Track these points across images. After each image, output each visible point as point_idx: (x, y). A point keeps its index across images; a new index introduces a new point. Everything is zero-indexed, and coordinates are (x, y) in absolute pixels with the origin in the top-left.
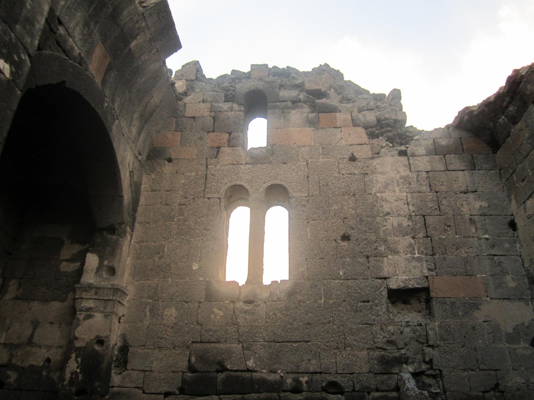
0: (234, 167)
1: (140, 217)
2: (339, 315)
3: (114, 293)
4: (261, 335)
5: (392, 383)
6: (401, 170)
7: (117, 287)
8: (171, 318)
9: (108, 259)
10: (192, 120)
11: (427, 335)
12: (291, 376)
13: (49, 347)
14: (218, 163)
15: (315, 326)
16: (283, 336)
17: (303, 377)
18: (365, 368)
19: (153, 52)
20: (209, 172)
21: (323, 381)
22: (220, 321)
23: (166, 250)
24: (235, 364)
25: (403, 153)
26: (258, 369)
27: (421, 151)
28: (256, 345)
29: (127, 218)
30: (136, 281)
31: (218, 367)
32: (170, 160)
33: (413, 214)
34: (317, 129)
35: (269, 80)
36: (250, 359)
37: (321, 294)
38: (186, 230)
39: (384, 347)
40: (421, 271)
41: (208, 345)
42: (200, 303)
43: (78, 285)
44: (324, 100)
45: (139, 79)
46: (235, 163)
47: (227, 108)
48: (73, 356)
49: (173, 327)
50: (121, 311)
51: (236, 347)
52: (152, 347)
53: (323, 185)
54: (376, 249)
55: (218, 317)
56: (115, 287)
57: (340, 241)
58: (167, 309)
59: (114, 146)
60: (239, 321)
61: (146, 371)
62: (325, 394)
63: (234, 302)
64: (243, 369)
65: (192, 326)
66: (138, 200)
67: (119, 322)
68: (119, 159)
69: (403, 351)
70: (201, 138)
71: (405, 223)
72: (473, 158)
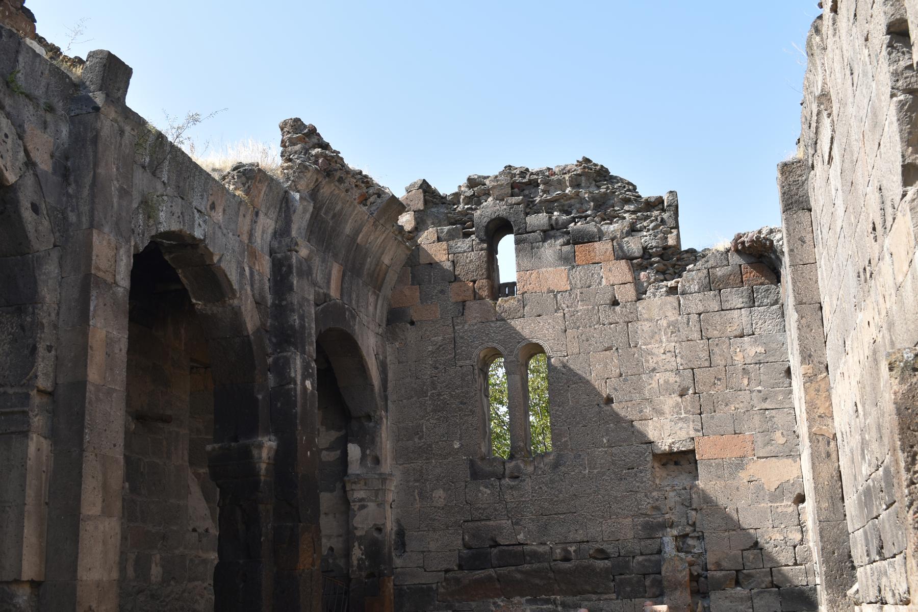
1: (392, 397)
5: (655, 547)
6: (669, 314)
11: (691, 498)
13: (329, 537)
18: (630, 535)
25: (672, 291)
26: (529, 542)
27: (695, 287)
31: (492, 543)
32: (412, 323)
33: (681, 368)
39: (649, 513)
40: (688, 433)
43: (346, 478)
45: (369, 260)
48: (356, 544)
49: (443, 508)
50: (390, 497)
51: (506, 523)
54: (641, 411)
62: (592, 561)
66: (386, 376)
68: (364, 353)
69: (667, 516)
70: (442, 292)
71: (672, 378)
72: (753, 291)
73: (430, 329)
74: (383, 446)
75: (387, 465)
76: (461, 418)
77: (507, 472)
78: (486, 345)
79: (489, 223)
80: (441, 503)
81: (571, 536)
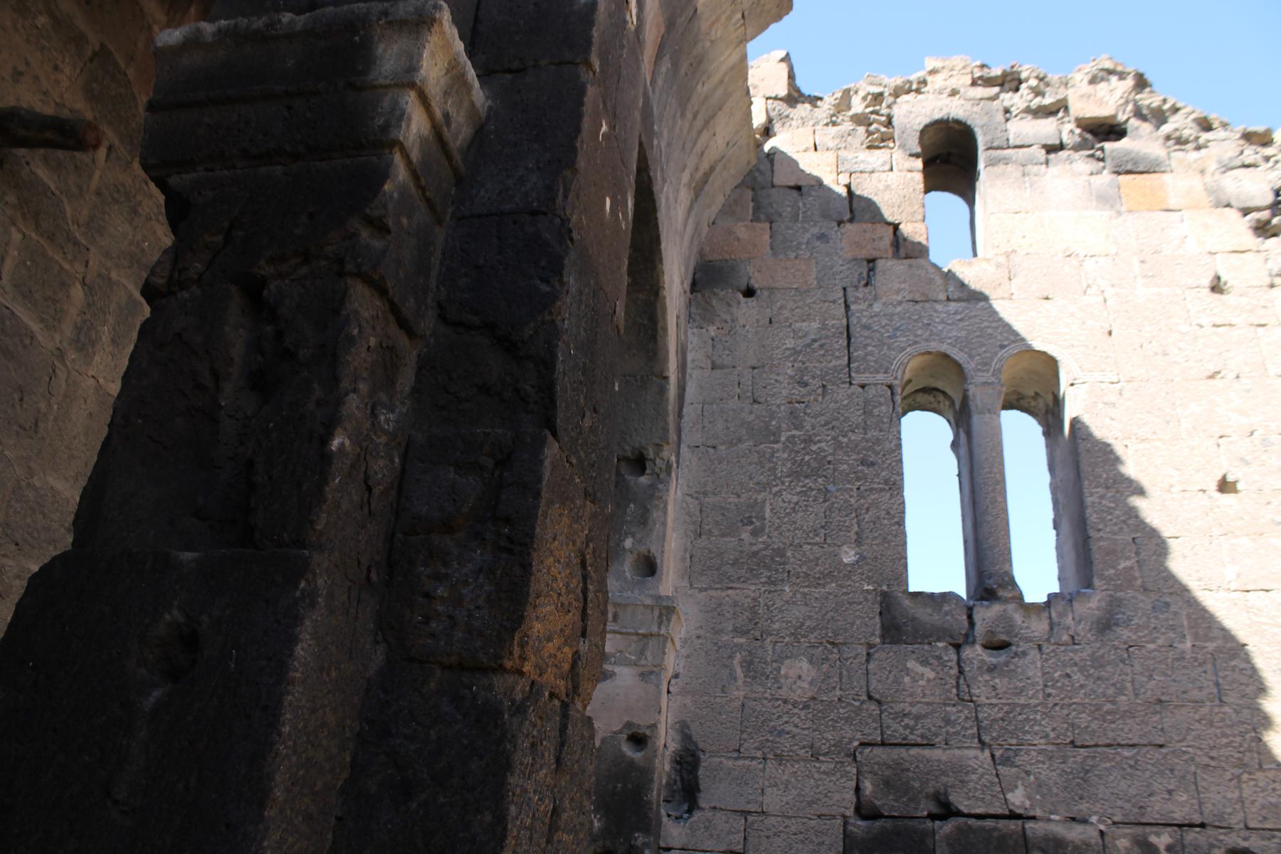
0: (918, 307)
2: (1234, 681)
3: (661, 615)
4: (1036, 728)
7: (670, 604)
8: (799, 683)
9: (634, 537)
10: (795, 193)
12: (1127, 831)
14: (876, 298)
15: (1176, 707)
16: (1093, 731)
17: (1158, 835)
19: (734, 20)
20: (853, 320)
21: (1212, 846)
22: (927, 692)
23: (768, 514)
24: (977, 799)
26: (1038, 813)
28: (1028, 752)
29: (673, 436)
30: (701, 590)
31: (934, 809)
32: (749, 293)
34: (1119, 213)
35: (979, 96)
36: (1016, 787)
37: (1182, 626)
38: (814, 464)
41: (903, 750)
42: (870, 646)
44: (1124, 143)
45: (700, 86)
46: (918, 298)
47: (881, 161)
49: (806, 707)
50: (672, 662)
52: (759, 754)
53: (1156, 354)
55: (922, 683)
56: (665, 604)
57: (1218, 495)
58: (787, 662)
59: (663, 246)
60: (975, 691)
61: (749, 812)
63: (958, 647)
64: (1000, 811)
65: (857, 704)
67: (669, 692)
68: (666, 278)
73: (791, 305)
74: (669, 531)
75: (669, 581)
76: (861, 496)
77: (979, 629)
78: (923, 347)
79: (926, 127)
80: (803, 691)
81: (1157, 809)
